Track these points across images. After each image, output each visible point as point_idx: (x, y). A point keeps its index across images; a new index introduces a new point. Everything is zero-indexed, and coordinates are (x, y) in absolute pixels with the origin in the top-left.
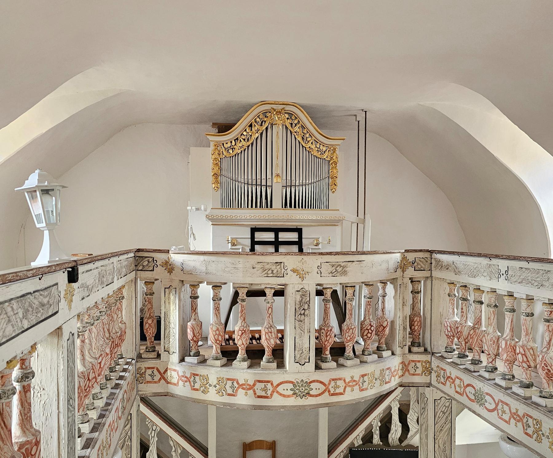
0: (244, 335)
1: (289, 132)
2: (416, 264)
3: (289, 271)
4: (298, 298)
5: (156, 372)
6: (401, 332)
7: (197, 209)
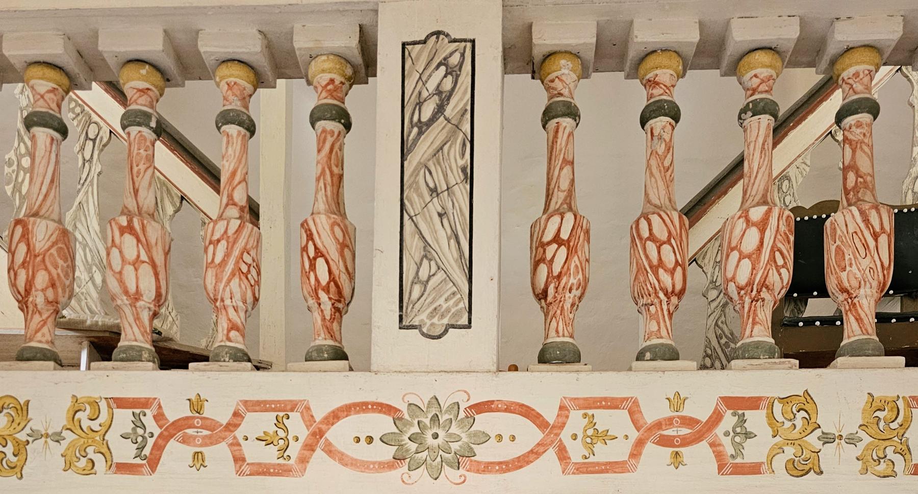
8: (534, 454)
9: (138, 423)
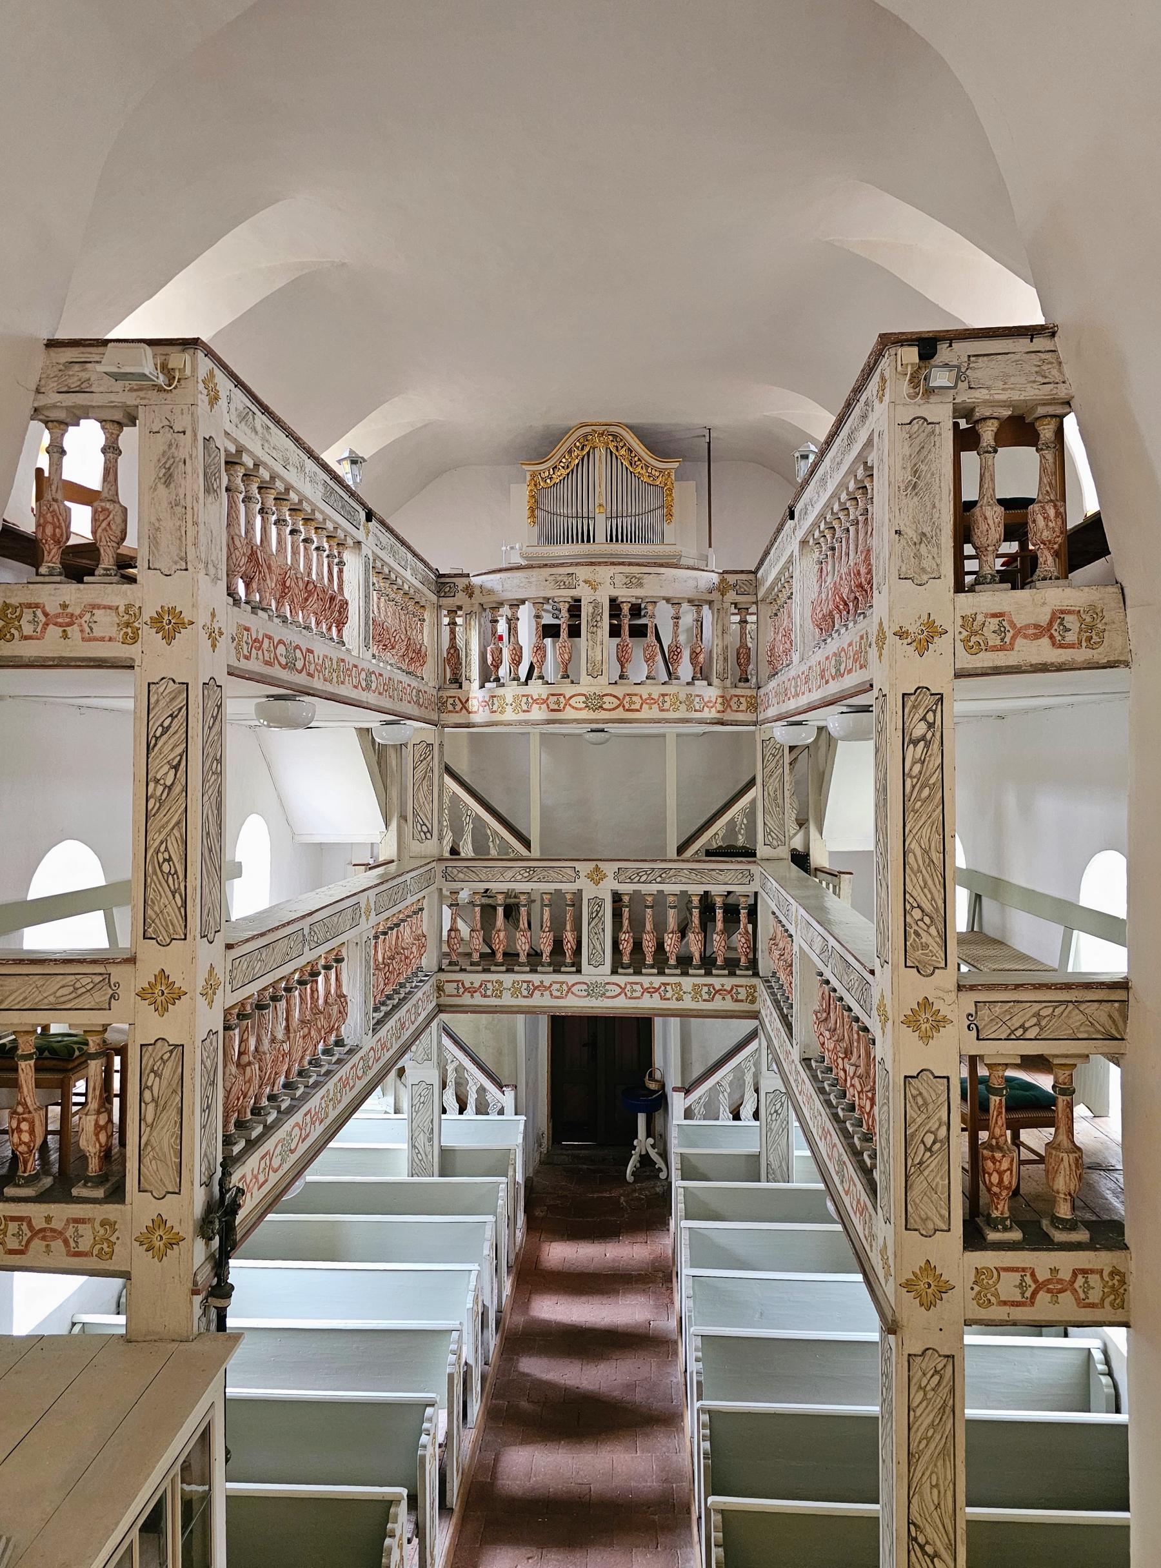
1: (614, 456)
3: (580, 582)
4: (591, 610)
6: (721, 662)
7: (512, 548)
8: (619, 994)
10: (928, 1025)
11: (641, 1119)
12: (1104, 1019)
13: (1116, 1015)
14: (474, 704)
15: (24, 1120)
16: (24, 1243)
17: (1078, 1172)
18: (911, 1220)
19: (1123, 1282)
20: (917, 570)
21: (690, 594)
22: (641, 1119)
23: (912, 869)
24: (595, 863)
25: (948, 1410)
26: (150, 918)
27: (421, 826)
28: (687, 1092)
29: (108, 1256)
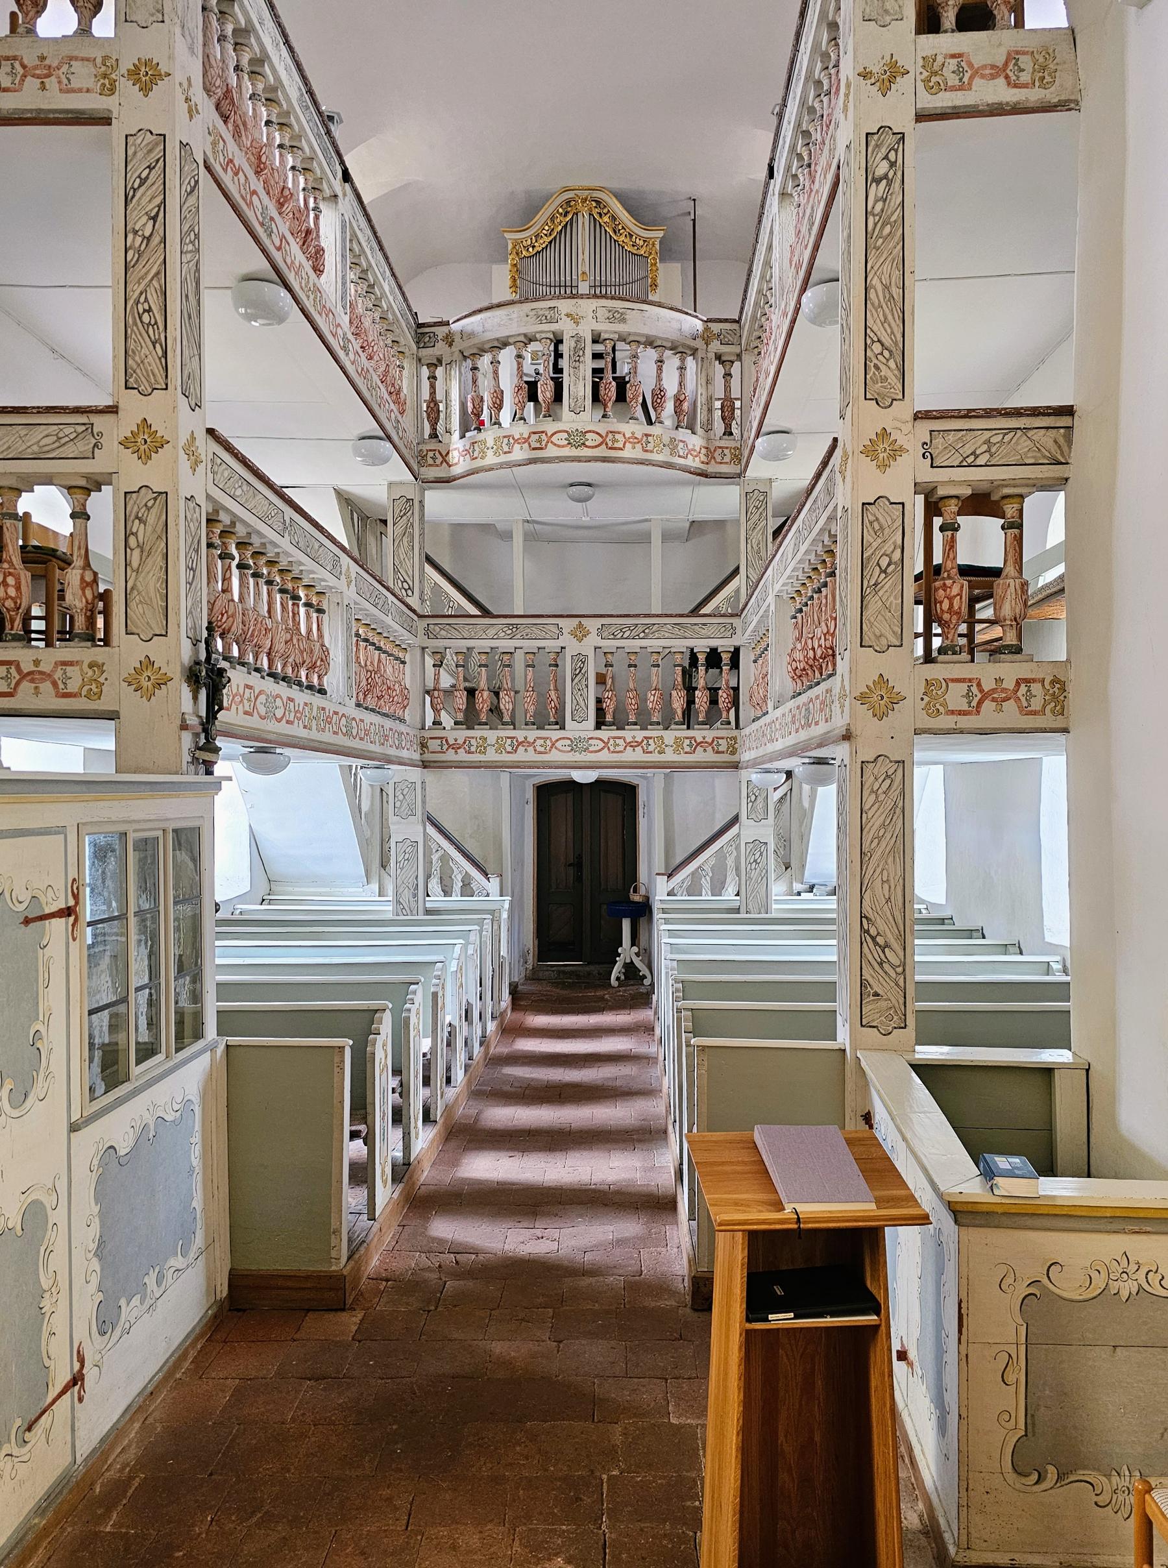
0: (520, 392)
2: (722, 337)
3: (562, 316)
4: (573, 344)
5: (437, 454)
6: (705, 413)
8: (603, 749)
9: (512, 742)
10: (885, 455)
11: (626, 925)
12: (1050, 444)
13: (1061, 441)
14: (454, 457)
15: (10, 574)
16: (12, 686)
17: (1024, 597)
18: (865, 638)
19: (1063, 690)
20: (880, 11)
21: (674, 336)
22: (626, 925)
23: (873, 304)
24: (579, 619)
25: (898, 811)
26: (132, 369)
27: (402, 582)
28: (670, 876)
29: (96, 697)
